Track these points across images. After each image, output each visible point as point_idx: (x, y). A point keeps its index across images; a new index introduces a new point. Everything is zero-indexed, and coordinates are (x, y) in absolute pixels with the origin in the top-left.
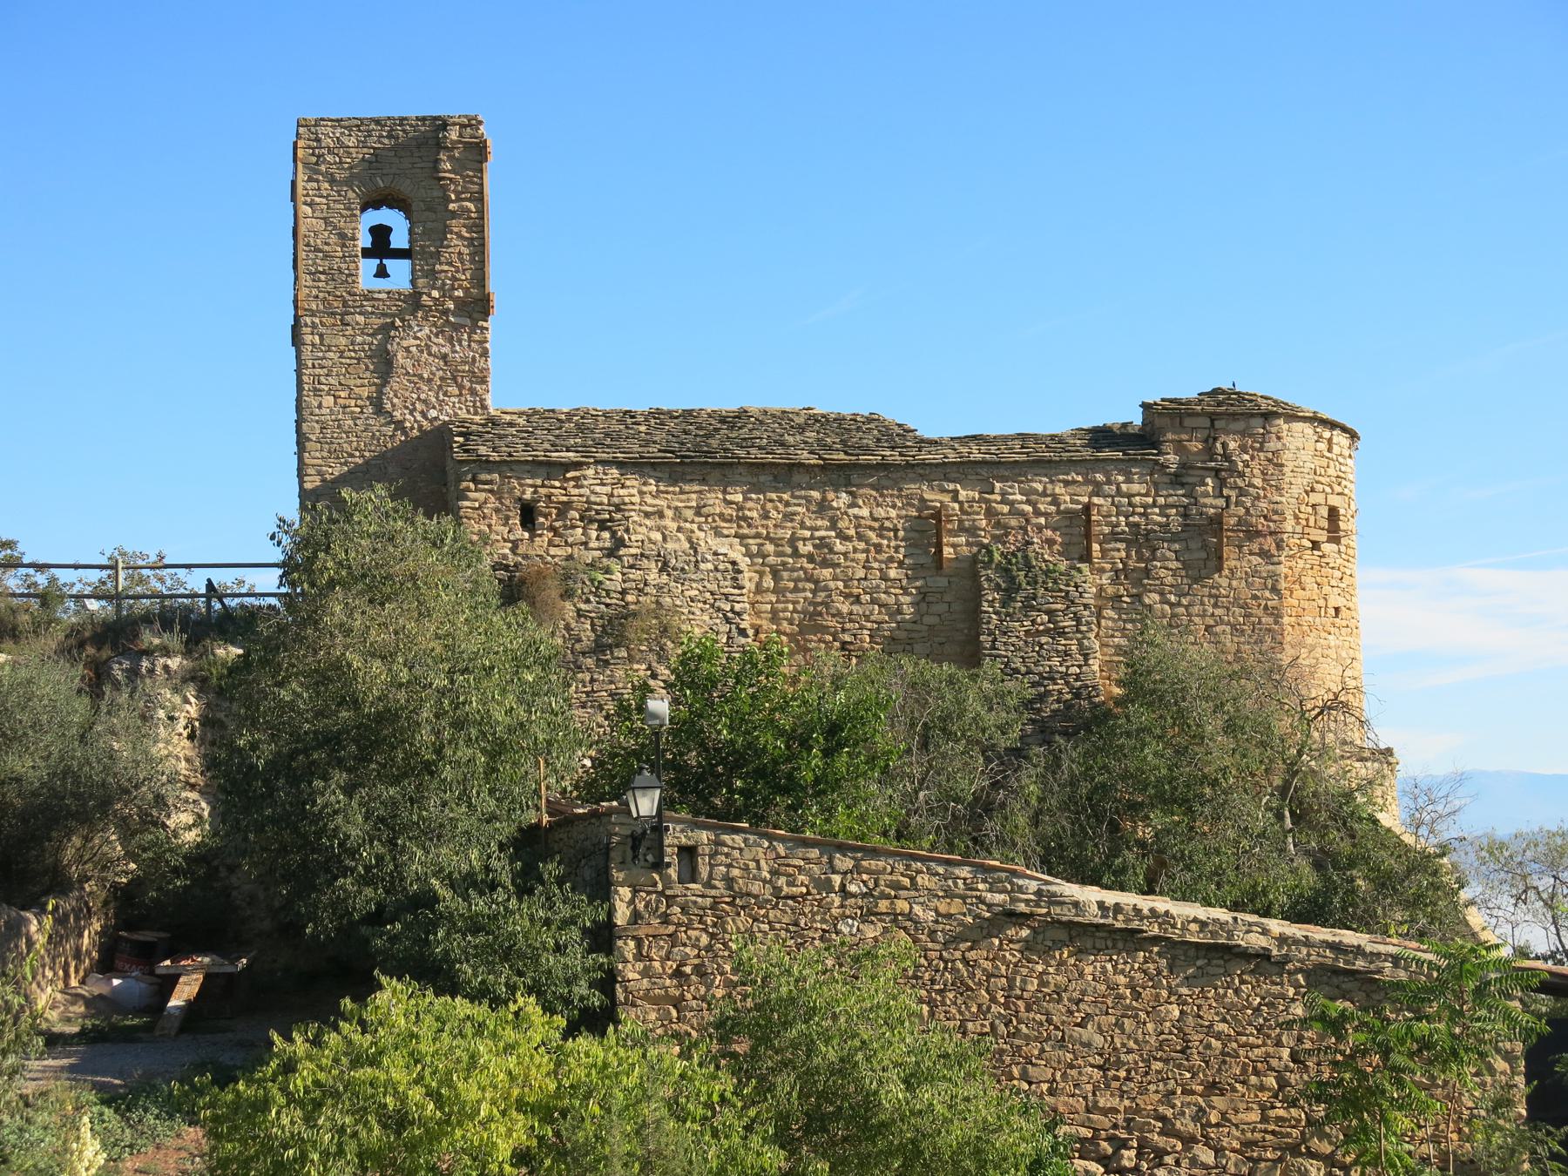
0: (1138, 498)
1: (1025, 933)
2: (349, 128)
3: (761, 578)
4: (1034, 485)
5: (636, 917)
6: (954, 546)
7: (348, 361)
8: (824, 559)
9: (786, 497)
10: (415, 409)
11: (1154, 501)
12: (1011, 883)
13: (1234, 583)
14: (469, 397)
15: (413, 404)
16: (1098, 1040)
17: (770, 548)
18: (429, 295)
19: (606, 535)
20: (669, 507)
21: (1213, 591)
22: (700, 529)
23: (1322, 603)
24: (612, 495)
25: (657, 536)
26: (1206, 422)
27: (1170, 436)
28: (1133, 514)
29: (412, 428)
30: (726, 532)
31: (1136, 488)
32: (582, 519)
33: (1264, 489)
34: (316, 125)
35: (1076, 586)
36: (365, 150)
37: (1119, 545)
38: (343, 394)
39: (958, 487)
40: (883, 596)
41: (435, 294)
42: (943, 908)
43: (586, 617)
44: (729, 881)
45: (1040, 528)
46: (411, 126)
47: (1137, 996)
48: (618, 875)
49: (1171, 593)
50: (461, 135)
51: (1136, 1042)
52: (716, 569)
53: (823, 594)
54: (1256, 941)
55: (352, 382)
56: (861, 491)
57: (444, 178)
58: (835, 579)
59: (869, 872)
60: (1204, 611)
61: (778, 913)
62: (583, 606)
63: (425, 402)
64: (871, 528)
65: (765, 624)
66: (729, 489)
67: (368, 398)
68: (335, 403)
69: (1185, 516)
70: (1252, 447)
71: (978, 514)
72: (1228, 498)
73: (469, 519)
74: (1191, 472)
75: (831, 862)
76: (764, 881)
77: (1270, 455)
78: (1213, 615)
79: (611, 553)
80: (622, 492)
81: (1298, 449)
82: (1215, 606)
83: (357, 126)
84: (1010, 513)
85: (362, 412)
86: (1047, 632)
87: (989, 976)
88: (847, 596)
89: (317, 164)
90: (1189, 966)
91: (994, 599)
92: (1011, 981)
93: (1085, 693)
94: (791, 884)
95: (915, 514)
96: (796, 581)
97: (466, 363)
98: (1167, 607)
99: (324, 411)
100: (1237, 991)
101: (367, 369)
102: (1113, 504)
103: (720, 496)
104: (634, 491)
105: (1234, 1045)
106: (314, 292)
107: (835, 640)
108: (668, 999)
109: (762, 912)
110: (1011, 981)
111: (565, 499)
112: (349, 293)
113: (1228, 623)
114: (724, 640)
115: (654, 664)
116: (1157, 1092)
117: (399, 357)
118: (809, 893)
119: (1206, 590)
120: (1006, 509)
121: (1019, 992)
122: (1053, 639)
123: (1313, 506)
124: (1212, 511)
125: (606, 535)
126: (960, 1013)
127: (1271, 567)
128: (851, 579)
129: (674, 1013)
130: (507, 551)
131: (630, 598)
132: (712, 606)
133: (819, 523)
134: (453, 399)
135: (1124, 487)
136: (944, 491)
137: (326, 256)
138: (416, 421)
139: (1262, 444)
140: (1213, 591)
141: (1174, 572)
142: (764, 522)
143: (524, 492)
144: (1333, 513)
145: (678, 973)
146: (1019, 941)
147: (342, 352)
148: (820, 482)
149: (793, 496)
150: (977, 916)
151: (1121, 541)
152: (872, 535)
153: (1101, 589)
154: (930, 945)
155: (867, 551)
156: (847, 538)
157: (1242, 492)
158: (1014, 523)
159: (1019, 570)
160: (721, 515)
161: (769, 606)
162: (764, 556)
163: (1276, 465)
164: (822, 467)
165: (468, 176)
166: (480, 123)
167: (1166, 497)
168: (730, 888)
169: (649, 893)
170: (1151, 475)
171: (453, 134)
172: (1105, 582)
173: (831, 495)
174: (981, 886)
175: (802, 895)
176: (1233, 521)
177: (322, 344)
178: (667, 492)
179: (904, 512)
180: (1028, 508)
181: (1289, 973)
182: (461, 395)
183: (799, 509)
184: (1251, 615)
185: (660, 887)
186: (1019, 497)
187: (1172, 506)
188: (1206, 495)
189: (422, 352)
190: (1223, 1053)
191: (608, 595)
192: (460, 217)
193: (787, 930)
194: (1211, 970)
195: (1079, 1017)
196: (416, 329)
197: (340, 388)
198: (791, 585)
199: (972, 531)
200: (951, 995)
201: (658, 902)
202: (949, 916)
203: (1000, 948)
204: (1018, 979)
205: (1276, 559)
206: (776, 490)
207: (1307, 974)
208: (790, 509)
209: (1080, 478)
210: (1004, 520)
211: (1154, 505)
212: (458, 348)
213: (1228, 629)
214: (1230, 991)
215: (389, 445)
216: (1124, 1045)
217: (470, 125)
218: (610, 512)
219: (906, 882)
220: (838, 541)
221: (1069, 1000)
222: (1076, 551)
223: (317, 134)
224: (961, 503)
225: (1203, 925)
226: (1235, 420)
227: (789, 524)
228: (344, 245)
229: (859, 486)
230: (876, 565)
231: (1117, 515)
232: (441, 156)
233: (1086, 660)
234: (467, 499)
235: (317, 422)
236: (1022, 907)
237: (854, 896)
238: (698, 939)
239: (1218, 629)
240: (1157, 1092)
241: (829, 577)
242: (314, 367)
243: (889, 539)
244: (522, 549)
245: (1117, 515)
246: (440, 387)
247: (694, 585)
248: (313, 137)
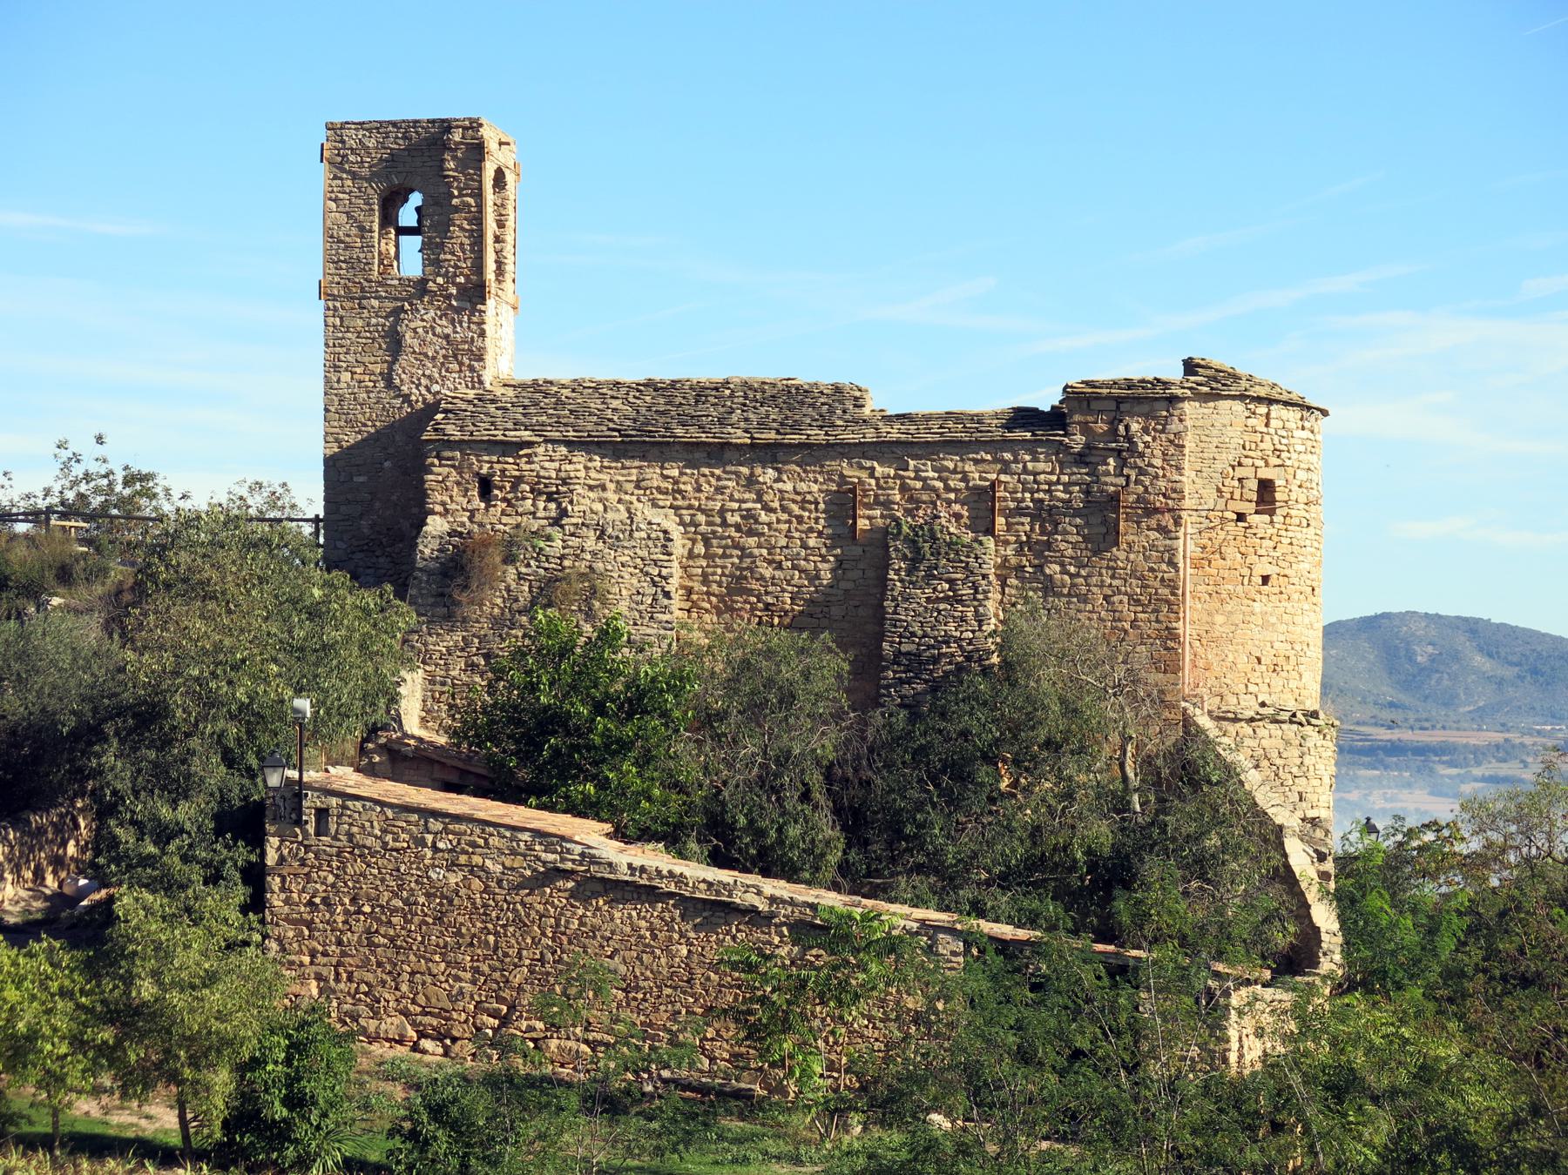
0: (1042, 476)
1: (570, 884)
3: (693, 544)
4: (945, 463)
5: (282, 860)
6: (870, 518)
8: (750, 529)
9: (717, 472)
10: (420, 384)
11: (1059, 479)
12: (561, 846)
13: (1132, 556)
14: (468, 374)
15: (419, 379)
16: (623, 969)
17: (701, 518)
19: (553, 506)
20: (611, 481)
21: (1111, 564)
22: (639, 500)
23: (1246, 572)
24: (560, 470)
25: (599, 507)
26: (1113, 406)
27: (1077, 418)
28: (1038, 491)
29: (417, 401)
30: (661, 503)
31: (1041, 466)
32: (532, 491)
33: (1163, 469)
34: (341, 129)
35: (977, 558)
37: (1023, 520)
38: (358, 370)
39: (876, 464)
40: (802, 563)
41: (440, 280)
42: (508, 864)
43: (525, 580)
44: (350, 836)
45: (949, 502)
47: (654, 937)
48: (270, 828)
49: (1071, 564)
50: (463, 137)
51: (652, 972)
52: (649, 538)
53: (749, 560)
54: (751, 899)
55: (366, 359)
56: (786, 467)
57: (448, 176)
58: (759, 546)
59: (454, 833)
60: (1102, 581)
61: (385, 862)
62: (523, 570)
63: (429, 377)
64: (794, 501)
65: (697, 586)
66: (666, 465)
67: (381, 374)
69: (1087, 493)
70: (1154, 429)
71: (893, 489)
72: (1128, 477)
74: (1094, 452)
75: (426, 823)
76: (376, 837)
77: (1172, 437)
78: (1110, 585)
79: (556, 522)
80: (569, 467)
81: (1225, 426)
82: (1113, 577)
83: (377, 128)
84: (923, 488)
85: (375, 387)
86: (946, 599)
87: (541, 916)
88: (770, 562)
89: (341, 163)
90: (697, 917)
91: (900, 568)
92: (558, 921)
93: (976, 656)
94: (395, 840)
95: (835, 488)
96: (726, 547)
98: (1066, 578)
100: (734, 938)
101: (380, 348)
102: (1019, 481)
103: (658, 471)
104: (580, 467)
105: (729, 979)
106: (337, 279)
107: (759, 601)
108: (302, 922)
109: (374, 860)
110: (558, 921)
111: (517, 473)
112: (366, 280)
113: (1126, 593)
114: (649, 602)
115: (581, 623)
116: (666, 1011)
118: (409, 847)
119: (1105, 563)
120: (919, 485)
121: (563, 929)
122: (952, 605)
123: (1240, 480)
124: (1112, 488)
125: (553, 506)
126: (518, 943)
127: (1168, 542)
128: (774, 547)
129: (306, 932)
130: (465, 519)
131: (567, 563)
132: (641, 571)
133: (747, 496)
134: (454, 375)
135: (1030, 466)
136: (861, 467)
139: (1164, 426)
140: (1111, 564)
141: (1075, 546)
142: (697, 495)
143: (481, 468)
144: (1266, 487)
145: (310, 903)
146: (566, 891)
147: (359, 333)
148: (750, 458)
149: (724, 472)
150: (535, 870)
151: (1025, 515)
152: (795, 509)
153: (1005, 559)
154: (497, 890)
155: (789, 522)
156: (773, 511)
157: (1142, 472)
158: (925, 498)
159: (925, 541)
160: (658, 489)
161: (700, 570)
162: (697, 525)
163: (1177, 446)
164: (752, 445)
166: (481, 125)
167: (1070, 475)
168: (350, 841)
169: (292, 843)
170: (1057, 454)
171: (457, 136)
172: (1009, 552)
173: (758, 470)
174: (537, 848)
175: (403, 849)
176: (1132, 498)
177: (341, 325)
178: (610, 468)
179: (825, 487)
180: (939, 485)
181: (776, 925)
182: (461, 371)
183: (730, 483)
184: (1147, 586)
185: (300, 838)
186: (931, 474)
187: (1076, 484)
188: (1107, 473)
189: (427, 332)
190: (719, 985)
191: (547, 560)
192: (461, 211)
193: (391, 875)
194: (714, 920)
195: (609, 951)
196: (423, 312)
198: (720, 551)
199: (887, 504)
200: (511, 929)
201: (298, 849)
202: (512, 869)
203: (551, 896)
204: (563, 919)
205: (1173, 535)
206: (709, 466)
207: (791, 927)
208: (721, 483)
209: (989, 457)
210: (916, 495)
211: (1058, 482)
212: (458, 329)
213: (1125, 599)
214: (728, 937)
215: (397, 417)
216: (642, 974)
217: (472, 128)
218: (557, 486)
219: (481, 842)
220: (763, 513)
221: (602, 937)
222: (982, 526)
224: (877, 479)
225: (710, 884)
226: (1139, 403)
227: (720, 497)
228: (362, 237)
229: (785, 463)
230: (797, 535)
231: (1023, 491)
232: (446, 156)
233: (980, 626)
234: (432, 473)
236: (569, 866)
237: (442, 851)
238: (325, 878)
239: (1116, 599)
240: (666, 1011)
241: (753, 545)
243: (810, 511)
244: (478, 517)
245: (1023, 491)
246: (443, 364)
247: (626, 552)
248: (338, 138)
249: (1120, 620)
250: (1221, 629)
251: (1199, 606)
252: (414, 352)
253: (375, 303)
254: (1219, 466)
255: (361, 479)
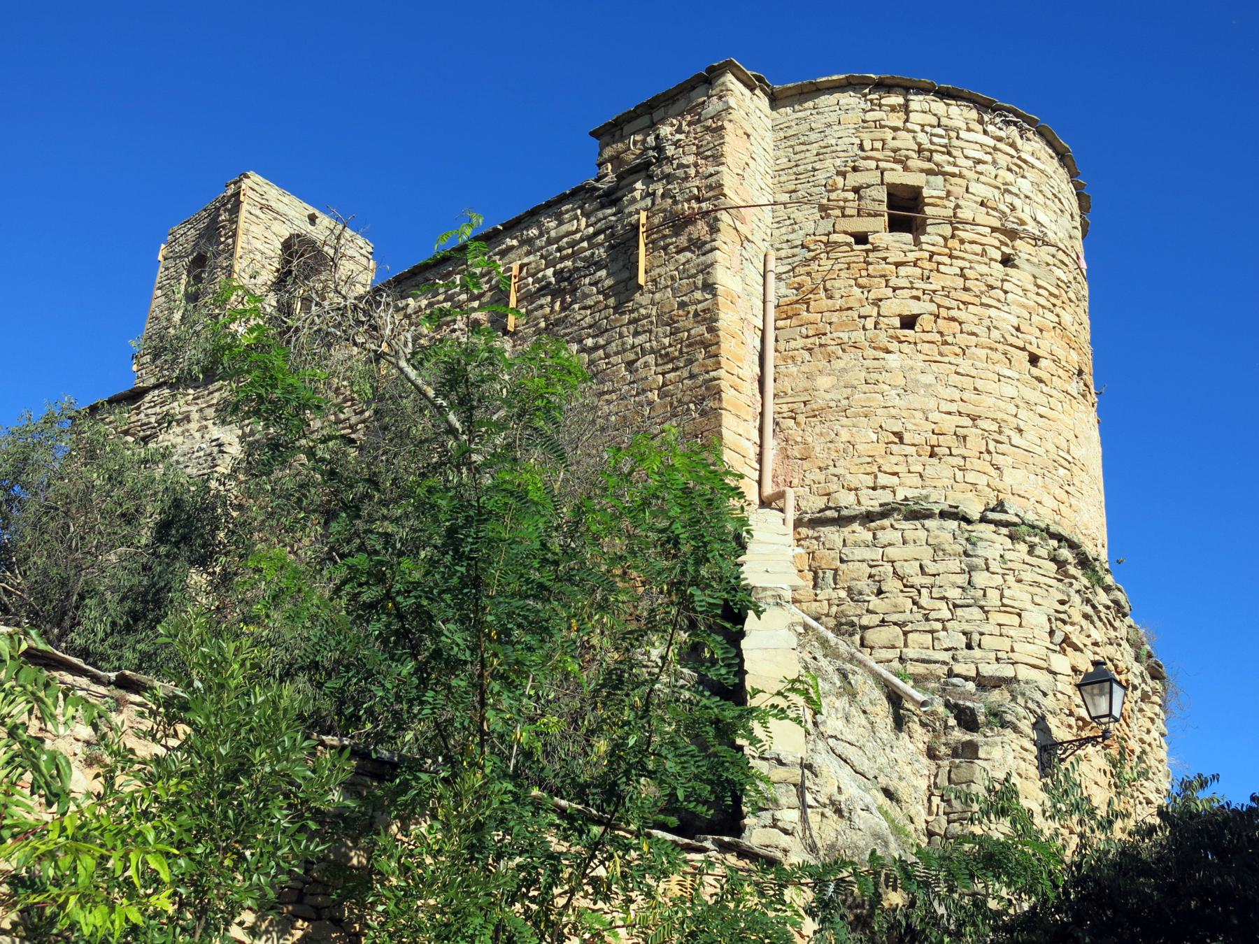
0: (565, 240)
22: (214, 424)
60: (623, 344)
78: (633, 347)
81: (830, 126)
82: (636, 334)
113: (652, 351)
119: (626, 318)
123: (856, 190)
127: (702, 258)
188: (634, 201)
205: (708, 247)
209: (515, 242)
213: (650, 359)
226: (674, 102)
249: (644, 391)
250: (828, 396)
251: (793, 369)
254: (821, 177)
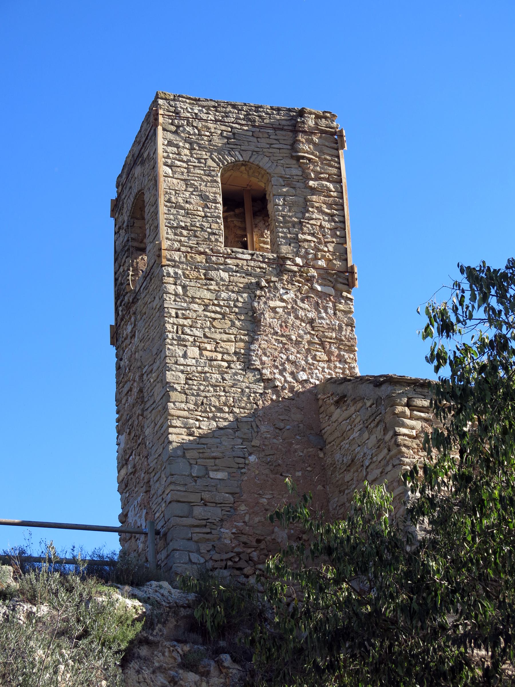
2: (208, 108)
7: (213, 315)
10: (285, 369)
14: (338, 365)
15: (283, 364)
18: (293, 261)
29: (283, 388)
34: (174, 100)
36: (223, 128)
38: (209, 347)
41: (299, 260)
46: (267, 113)
55: (218, 336)
57: (303, 157)
63: (293, 363)
67: (236, 353)
68: (201, 354)
73: (408, 447)
83: (214, 107)
85: (229, 367)
97: (333, 330)
99: (190, 362)
101: (233, 325)
117: (267, 316)
134: (321, 364)
137: (188, 214)
138: (286, 381)
147: (206, 305)
165: (326, 159)
189: (289, 314)
197: (206, 340)
212: (324, 315)
215: (260, 402)
223: (176, 107)
234: (404, 425)
235: (182, 372)
242: (177, 317)
246: (308, 351)
248: (173, 109)
252: (276, 333)
253: (225, 275)
255: (220, 475)
